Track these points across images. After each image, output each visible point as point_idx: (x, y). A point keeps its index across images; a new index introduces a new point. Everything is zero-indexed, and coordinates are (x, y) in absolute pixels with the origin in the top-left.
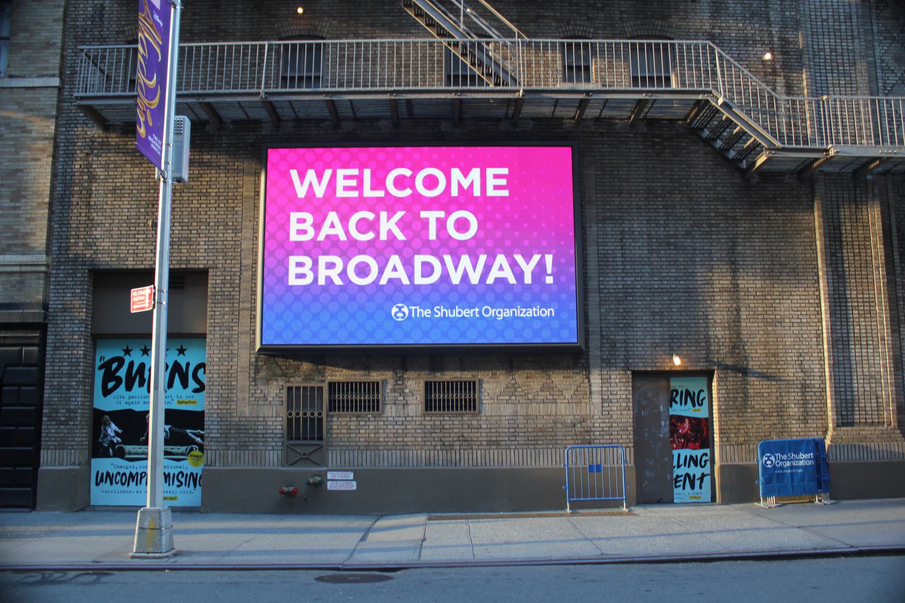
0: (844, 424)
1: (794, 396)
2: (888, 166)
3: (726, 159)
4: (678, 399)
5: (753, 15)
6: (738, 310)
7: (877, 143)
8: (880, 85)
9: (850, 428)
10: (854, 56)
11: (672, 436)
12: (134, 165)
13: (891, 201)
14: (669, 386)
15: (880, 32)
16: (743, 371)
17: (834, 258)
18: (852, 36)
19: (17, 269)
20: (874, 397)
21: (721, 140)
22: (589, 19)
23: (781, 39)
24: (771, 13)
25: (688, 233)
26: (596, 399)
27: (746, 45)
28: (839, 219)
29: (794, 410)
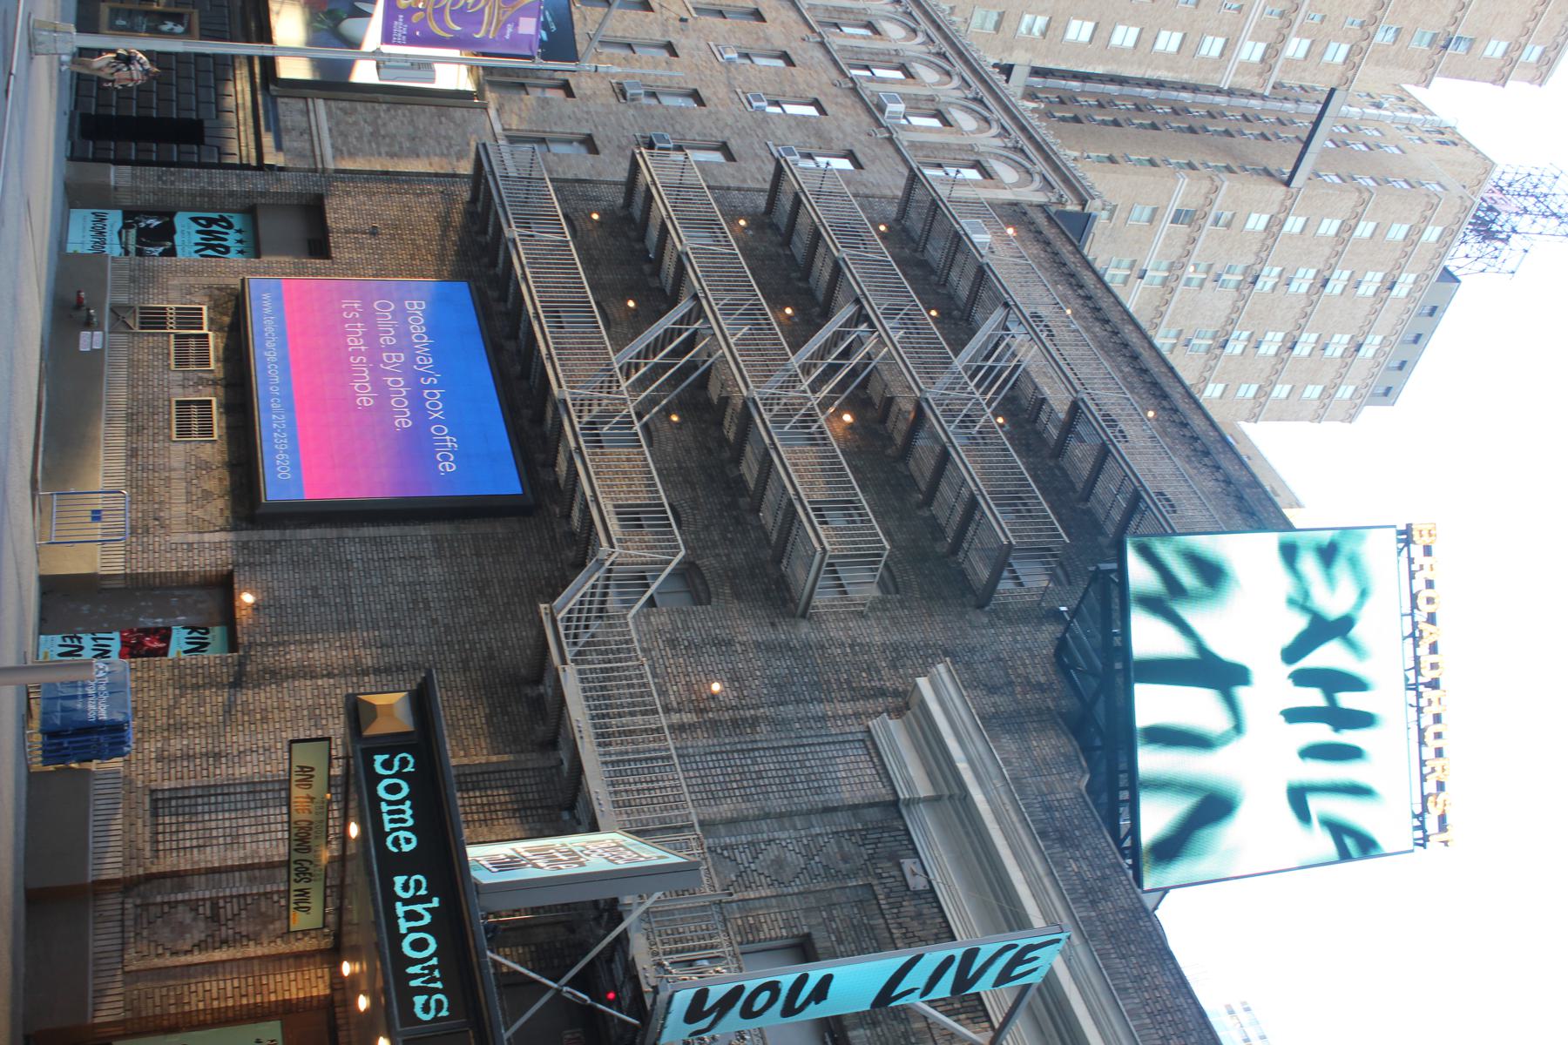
0: (154, 801)
1: (199, 744)
4: (195, 634)
6: (330, 675)
9: (147, 807)
11: (139, 630)
12: (437, 219)
14: (214, 625)
16: (238, 683)
19: (318, 152)
20: (201, 842)
22: (706, 528)
25: (434, 621)
26: (193, 538)
27: (731, 680)
28: (491, 788)
29: (177, 745)
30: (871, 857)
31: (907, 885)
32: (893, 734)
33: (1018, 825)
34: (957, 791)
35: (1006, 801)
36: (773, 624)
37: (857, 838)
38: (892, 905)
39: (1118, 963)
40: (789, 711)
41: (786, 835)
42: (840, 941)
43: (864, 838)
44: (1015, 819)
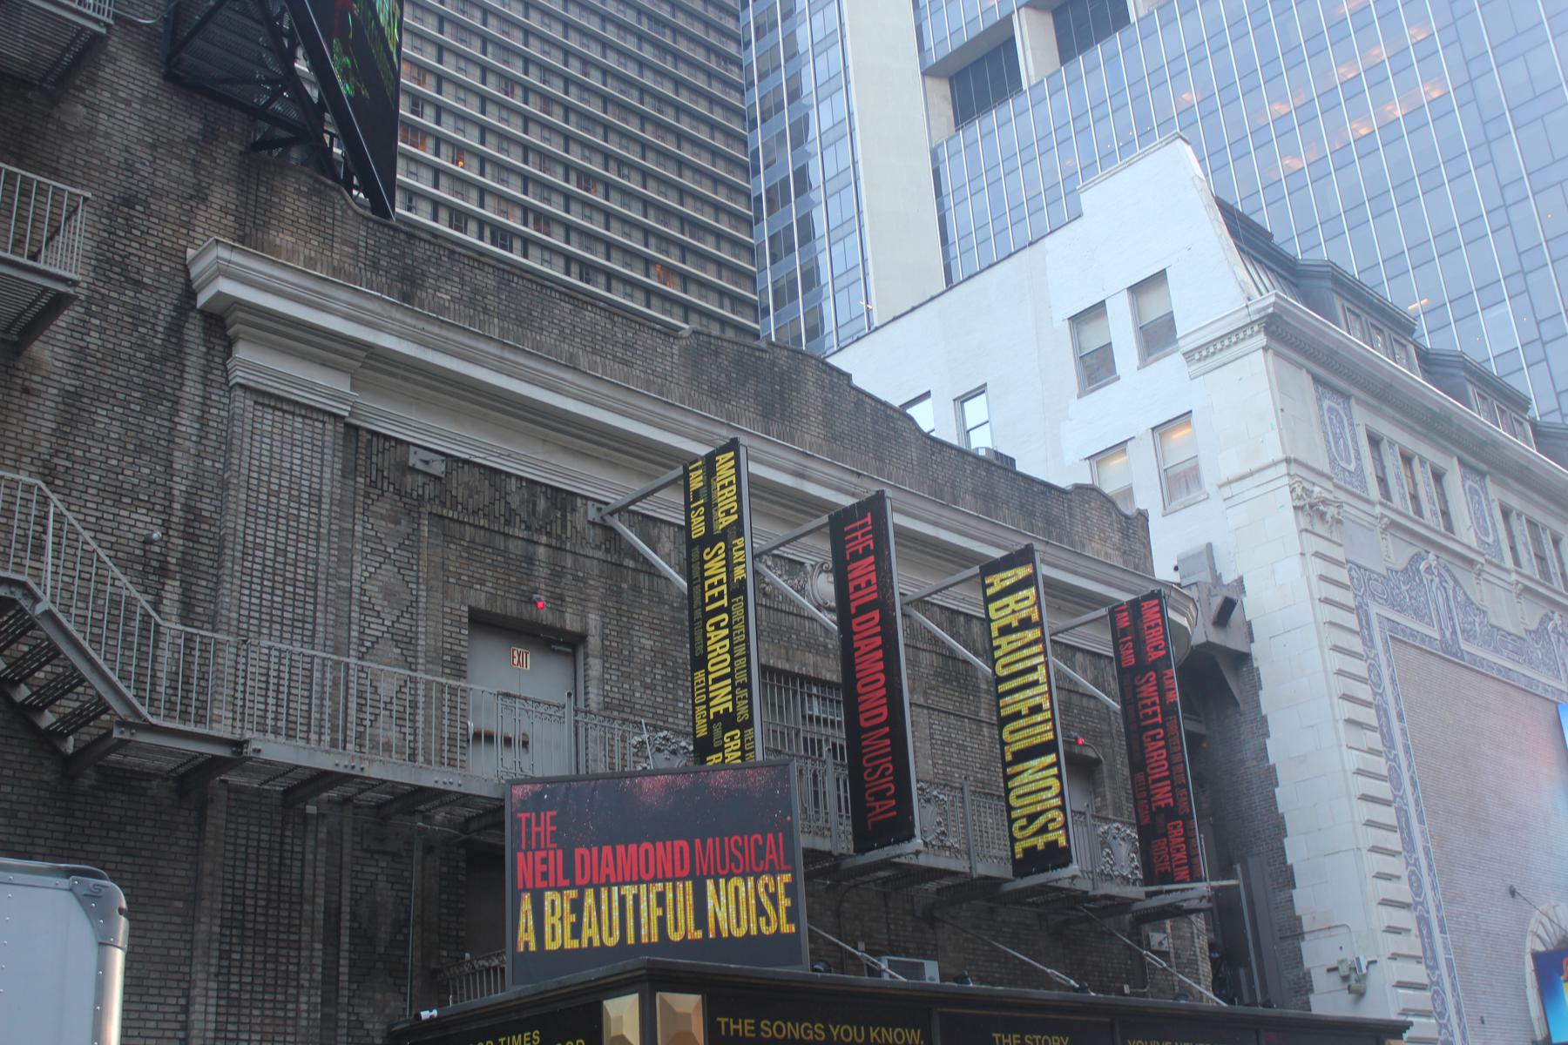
2: (349, 790)
3: (33, 728)
5: (141, 449)
7: (334, 744)
8: (355, 634)
10: (316, 571)
13: (346, 859)
15: (365, 538)
17: (225, 963)
18: (318, 533)
21: (28, 685)
23: (187, 508)
24: (176, 453)
30: (397, 492)
31: (437, 478)
32: (253, 360)
33: (444, 333)
34: (363, 354)
35: (412, 321)
36: (26, 391)
37: (374, 493)
38: (454, 508)
39: (547, 339)
40: (180, 461)
41: (357, 571)
42: (483, 583)
43: (373, 484)
44: (436, 330)
